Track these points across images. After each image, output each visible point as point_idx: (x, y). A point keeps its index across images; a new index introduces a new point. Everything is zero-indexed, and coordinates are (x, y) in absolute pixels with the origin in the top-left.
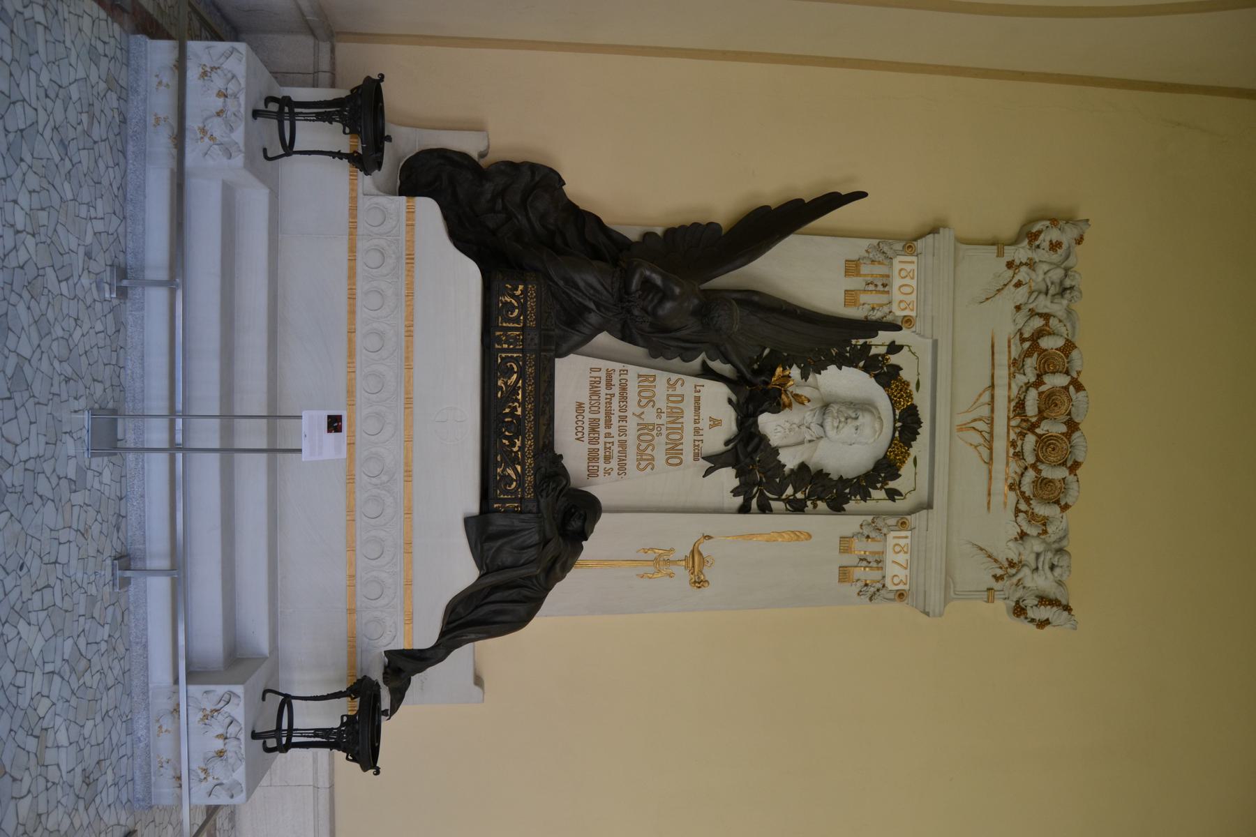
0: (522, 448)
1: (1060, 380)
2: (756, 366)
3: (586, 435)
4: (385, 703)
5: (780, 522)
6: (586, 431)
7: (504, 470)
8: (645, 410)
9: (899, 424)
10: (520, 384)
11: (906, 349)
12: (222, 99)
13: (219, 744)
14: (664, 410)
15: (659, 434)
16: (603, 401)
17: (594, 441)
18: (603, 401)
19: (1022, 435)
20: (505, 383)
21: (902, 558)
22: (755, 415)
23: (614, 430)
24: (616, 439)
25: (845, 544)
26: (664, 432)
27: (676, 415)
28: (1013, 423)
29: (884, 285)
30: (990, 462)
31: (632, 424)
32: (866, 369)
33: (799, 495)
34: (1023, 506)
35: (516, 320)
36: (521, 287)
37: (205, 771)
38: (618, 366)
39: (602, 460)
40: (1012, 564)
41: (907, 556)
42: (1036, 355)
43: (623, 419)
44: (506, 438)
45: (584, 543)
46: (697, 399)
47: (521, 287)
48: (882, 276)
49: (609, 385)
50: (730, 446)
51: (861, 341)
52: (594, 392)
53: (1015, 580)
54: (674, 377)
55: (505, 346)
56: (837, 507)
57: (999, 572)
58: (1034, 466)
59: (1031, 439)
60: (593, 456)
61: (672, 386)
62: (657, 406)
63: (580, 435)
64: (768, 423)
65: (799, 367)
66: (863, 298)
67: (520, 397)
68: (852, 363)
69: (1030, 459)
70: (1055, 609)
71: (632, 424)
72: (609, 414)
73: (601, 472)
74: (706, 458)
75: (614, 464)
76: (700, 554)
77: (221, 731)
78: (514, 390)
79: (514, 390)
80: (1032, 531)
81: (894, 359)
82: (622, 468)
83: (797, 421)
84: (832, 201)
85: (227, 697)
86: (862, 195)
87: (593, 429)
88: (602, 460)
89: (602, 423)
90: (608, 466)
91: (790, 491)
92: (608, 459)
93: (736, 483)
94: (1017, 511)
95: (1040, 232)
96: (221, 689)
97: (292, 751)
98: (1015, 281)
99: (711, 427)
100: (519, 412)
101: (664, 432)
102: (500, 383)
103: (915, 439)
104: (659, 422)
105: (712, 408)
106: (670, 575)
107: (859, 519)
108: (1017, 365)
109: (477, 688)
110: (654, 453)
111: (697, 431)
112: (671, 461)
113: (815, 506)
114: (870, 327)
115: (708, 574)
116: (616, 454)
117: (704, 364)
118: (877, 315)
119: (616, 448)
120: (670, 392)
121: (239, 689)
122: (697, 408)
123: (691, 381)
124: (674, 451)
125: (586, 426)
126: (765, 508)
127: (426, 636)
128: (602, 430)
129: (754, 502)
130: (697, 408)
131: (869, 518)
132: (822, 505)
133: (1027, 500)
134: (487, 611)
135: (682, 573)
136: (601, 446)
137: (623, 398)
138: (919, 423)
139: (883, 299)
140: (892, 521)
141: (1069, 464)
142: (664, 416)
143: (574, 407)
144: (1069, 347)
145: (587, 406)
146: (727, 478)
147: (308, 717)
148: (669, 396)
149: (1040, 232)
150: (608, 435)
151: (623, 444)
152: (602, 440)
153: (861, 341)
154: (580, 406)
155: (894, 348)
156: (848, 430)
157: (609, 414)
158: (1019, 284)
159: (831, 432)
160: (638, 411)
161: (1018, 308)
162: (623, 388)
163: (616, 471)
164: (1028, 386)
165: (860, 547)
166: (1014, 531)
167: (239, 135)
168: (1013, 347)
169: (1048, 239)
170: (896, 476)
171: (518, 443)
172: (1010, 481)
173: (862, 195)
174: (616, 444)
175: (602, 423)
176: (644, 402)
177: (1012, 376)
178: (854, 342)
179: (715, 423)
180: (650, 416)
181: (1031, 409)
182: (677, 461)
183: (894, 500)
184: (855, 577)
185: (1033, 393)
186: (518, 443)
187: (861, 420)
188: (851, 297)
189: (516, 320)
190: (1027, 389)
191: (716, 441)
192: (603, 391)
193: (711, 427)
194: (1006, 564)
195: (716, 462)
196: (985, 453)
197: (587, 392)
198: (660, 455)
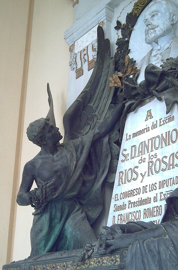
14: (140, 158)
23: (151, 195)
31: (149, 181)
62: (137, 164)
72: (142, 202)
89: (146, 206)
101: (155, 151)
110: (168, 155)
142: (144, 156)
157: (142, 202)
160: (140, 177)
173: (48, 84)
174: (162, 190)
180: (143, 168)
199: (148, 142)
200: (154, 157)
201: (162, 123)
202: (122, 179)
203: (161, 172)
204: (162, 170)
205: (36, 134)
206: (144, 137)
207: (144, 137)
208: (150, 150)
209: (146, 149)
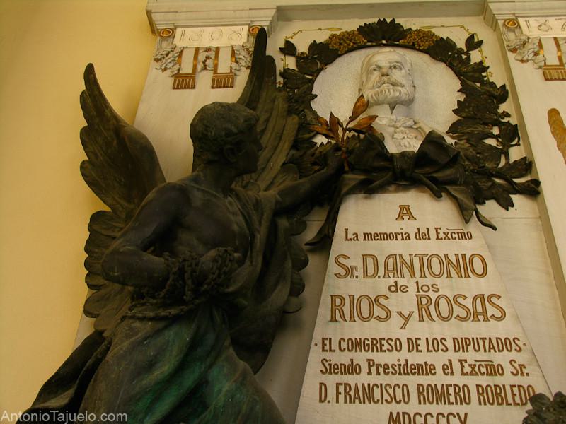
3: (454, 409)
5: (540, 143)
6: (446, 409)
8: (394, 310)
9: (384, 42)
14: (392, 281)
15: (435, 288)
17: (462, 395)
18: (383, 379)
23: (438, 359)
24: (455, 357)
26: (429, 281)
27: (397, 265)
31: (422, 330)
33: (496, 131)
38: (315, 356)
39: (498, 380)
43: (413, 345)
46: (368, 237)
49: (353, 369)
51: (280, 79)
52: (367, 394)
54: (333, 268)
61: (349, 271)
62: (385, 292)
64: (401, 141)
71: (422, 330)
72: (407, 369)
73: (518, 380)
82: (505, 344)
83: (392, 130)
87: (440, 395)
88: (498, 380)
89: (425, 380)
90: (508, 369)
91: (491, 142)
92: (494, 370)
99: (412, 217)
101: (429, 281)
104: (412, 290)
111: (420, 236)
112: (479, 269)
114: (260, 63)
116: (482, 356)
118: (246, 60)
119: (471, 356)
120: (360, 273)
124: (463, 266)
125: (435, 408)
126: (526, 165)
128: (439, 379)
136: (472, 382)
137: (375, 344)
142: (401, 282)
148: (366, 275)
150: (448, 370)
151: (462, 344)
152: (458, 379)
153: (280, 79)
155: (289, 49)
157: (407, 369)
159: (403, 92)
160: (396, 321)
162: (357, 345)
163: (513, 355)
174: (461, 355)
175: (425, 380)
176: (378, 311)
179: (405, 212)
180: (406, 301)
183: (480, 43)
191: (433, 212)
192: (363, 379)
193: (412, 217)
198: (472, 287)
200: (431, 289)
202: (342, 313)
203: (453, 319)
204: (455, 318)
205: (235, 131)
206: (383, 249)
207: (383, 249)
208: (418, 273)
209: (405, 270)
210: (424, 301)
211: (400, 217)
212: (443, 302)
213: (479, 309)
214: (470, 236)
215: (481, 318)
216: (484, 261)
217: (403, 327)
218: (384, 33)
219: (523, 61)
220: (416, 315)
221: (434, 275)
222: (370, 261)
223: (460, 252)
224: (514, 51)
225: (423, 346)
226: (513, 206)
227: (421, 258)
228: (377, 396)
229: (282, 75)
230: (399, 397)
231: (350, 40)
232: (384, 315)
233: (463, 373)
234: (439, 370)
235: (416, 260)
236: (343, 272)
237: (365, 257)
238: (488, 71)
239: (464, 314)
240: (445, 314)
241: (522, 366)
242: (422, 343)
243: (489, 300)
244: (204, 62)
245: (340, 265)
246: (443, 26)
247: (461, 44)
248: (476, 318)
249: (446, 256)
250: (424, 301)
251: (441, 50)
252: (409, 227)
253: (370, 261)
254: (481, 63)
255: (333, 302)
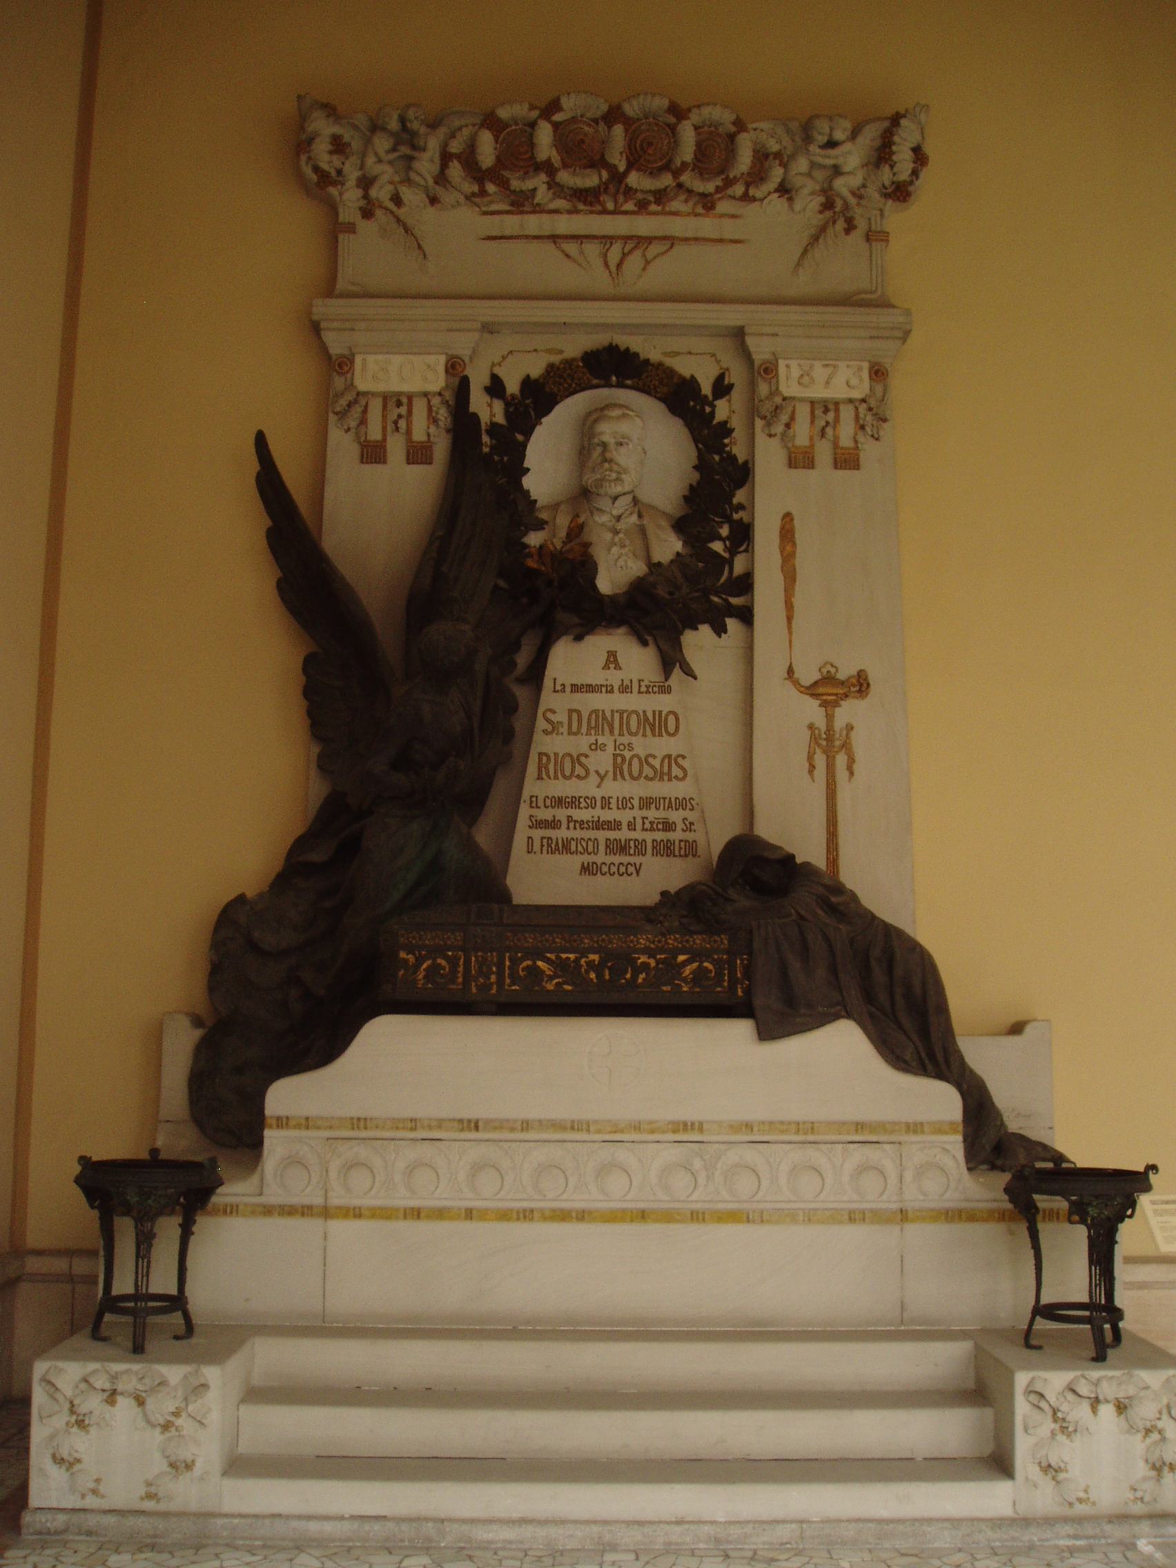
0: (651, 953)
1: (544, 135)
2: (525, 600)
3: (632, 859)
4: (1050, 1165)
6: (625, 859)
7: (685, 980)
8: (592, 768)
10: (552, 956)
11: (497, 370)
12: (119, 1399)
13: (1107, 1411)
16: (578, 834)
17: (640, 848)
18: (578, 834)
19: (629, 192)
20: (551, 978)
21: (819, 372)
22: (598, 598)
23: (624, 816)
24: (637, 813)
25: (800, 460)
26: (626, 739)
27: (600, 722)
28: (610, 206)
29: (399, 404)
30: (671, 241)
31: (614, 789)
32: (528, 433)
33: (725, 531)
34: (739, 190)
35: (453, 962)
36: (403, 955)
37: (1148, 1431)
38: (524, 812)
39: (671, 836)
40: (828, 205)
41: (818, 365)
42: (506, 174)
43: (606, 803)
44: (635, 977)
45: (799, 860)
46: (576, 688)
47: (403, 955)
48: (385, 407)
49: (554, 824)
50: (649, 638)
51: (486, 439)
53: (852, 201)
54: (541, 724)
55: (493, 978)
56: (742, 474)
57: (841, 224)
58: (676, 174)
59: (633, 179)
60: (665, 849)
62: (585, 749)
63: (631, 869)
65: (525, 534)
66: (419, 435)
67: (572, 956)
68: (519, 451)
69: (667, 180)
70: (896, 139)
71: (614, 789)
73: (690, 836)
74: (667, 673)
75: (676, 816)
76: (816, 683)
77: (1085, 1407)
78: (561, 967)
79: (561, 967)
80: (777, 173)
81: (512, 386)
82: (682, 804)
83: (609, 536)
84: (270, 483)
85: (1033, 1398)
86: (261, 440)
87: (622, 848)
88: (671, 836)
89: (612, 835)
90: (680, 826)
91: (717, 546)
92: (668, 826)
93: (705, 630)
94: (746, 198)
95: (316, 169)
96: (1022, 1406)
97: (1119, 1302)
98: (391, 206)
99: (618, 667)
100: (595, 957)
101: (626, 739)
102: (550, 986)
103: (636, 355)
104: (610, 749)
105: (589, 669)
106: (850, 728)
107: (761, 439)
108: (522, 203)
109: (1029, 1029)
110: (660, 754)
111: (625, 689)
112: (671, 728)
113: (741, 507)
114: (463, 423)
115: (846, 671)
117: (521, 680)
118: (443, 414)
119: (652, 814)
120: (564, 730)
121: (1022, 1379)
122: (591, 688)
123: (548, 699)
124: (657, 724)
125: (617, 859)
126: (745, 584)
127: (943, 1101)
128: (624, 834)
129: (734, 601)
130: (591, 688)
131: (759, 423)
132: (740, 496)
133: (729, 183)
134: (905, 1009)
135: (846, 712)
136: (649, 837)
137: (574, 802)
138: (612, 349)
139: (420, 408)
140: (763, 389)
141: (672, 120)
143: (587, 879)
144: (491, 122)
145: (587, 859)
146: (699, 642)
147: (1070, 1280)
149: (316, 169)
150: (631, 826)
151: (646, 803)
153: (486, 439)
154: (586, 869)
155: (495, 388)
156: (623, 457)
157: (599, 825)
158: (397, 200)
160: (593, 779)
161: (433, 200)
162: (559, 802)
164: (552, 185)
165: (802, 433)
166: (777, 204)
167: (174, 1373)
168: (494, 207)
169: (326, 157)
170: (691, 385)
171: (643, 959)
172: (700, 210)
173: (261, 440)
174: (644, 813)
175: (612, 835)
176: (579, 770)
177: (538, 210)
178: (486, 450)
179: (612, 660)
180: (602, 761)
181: (591, 180)
182: (671, 719)
183: (731, 386)
184: (852, 445)
185: (564, 177)
186: (643, 959)
187: (605, 438)
188: (418, 454)
189: (453, 962)
190: (558, 184)
191: (639, 661)
192: (563, 833)
193: (618, 667)
194: (828, 214)
195: (671, 660)
196: (654, 249)
197: (564, 859)
198: (662, 746)
199: (613, 716)
201: (643, 689)
208: (616, 732)
210: (619, 759)
211: (606, 667)
212: (635, 762)
213: (666, 769)
214: (668, 690)
215: (666, 778)
216: (677, 719)
217: (598, 786)
218: (613, 366)
219: (770, 436)
220: (611, 775)
221: (631, 734)
222: (575, 716)
223: (658, 709)
224: (764, 418)
225: (613, 805)
226: (725, 632)
227: (621, 713)
228: (573, 848)
229: (488, 432)
230: (590, 849)
231: (573, 380)
232: (583, 773)
233: (643, 829)
234: (625, 826)
235: (617, 716)
236: (550, 728)
237: (571, 711)
238: (734, 435)
239: (651, 774)
240: (635, 774)
241: (692, 824)
242: (613, 801)
243: (676, 763)
244: (396, 423)
245: (548, 720)
246: (690, 353)
247: (706, 389)
248: (661, 779)
249: (644, 712)
250: (619, 759)
251: (682, 398)
252: (614, 677)
253: (575, 716)
254: (726, 422)
255: (540, 760)
